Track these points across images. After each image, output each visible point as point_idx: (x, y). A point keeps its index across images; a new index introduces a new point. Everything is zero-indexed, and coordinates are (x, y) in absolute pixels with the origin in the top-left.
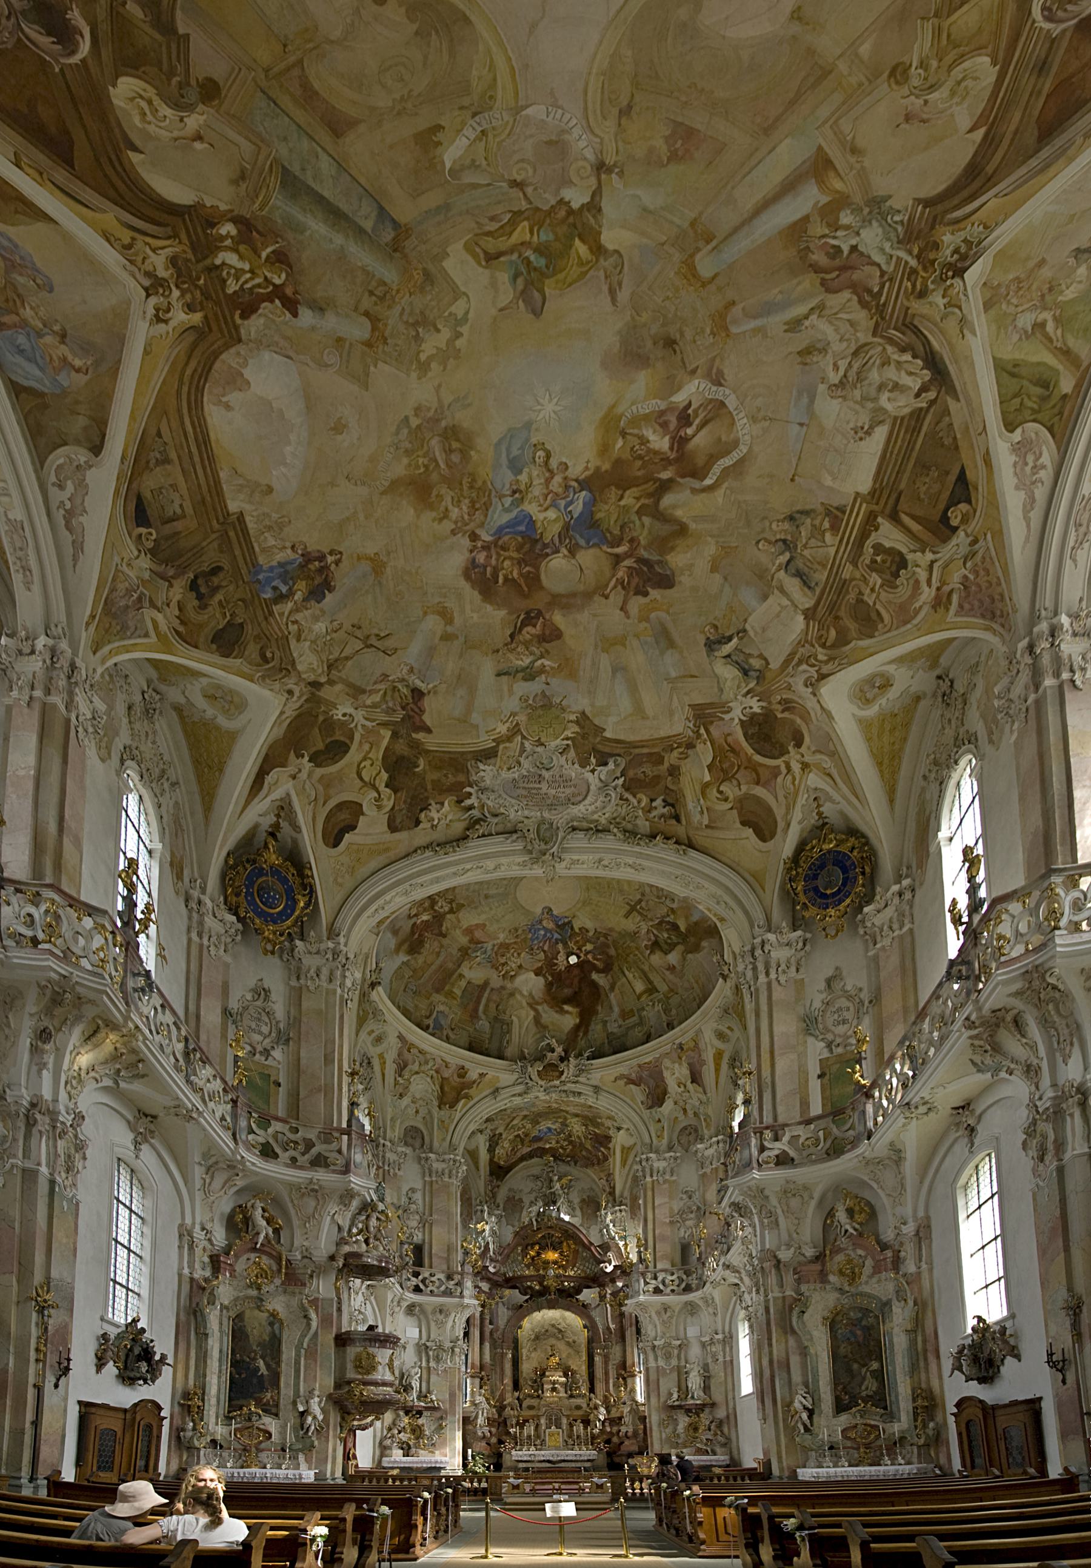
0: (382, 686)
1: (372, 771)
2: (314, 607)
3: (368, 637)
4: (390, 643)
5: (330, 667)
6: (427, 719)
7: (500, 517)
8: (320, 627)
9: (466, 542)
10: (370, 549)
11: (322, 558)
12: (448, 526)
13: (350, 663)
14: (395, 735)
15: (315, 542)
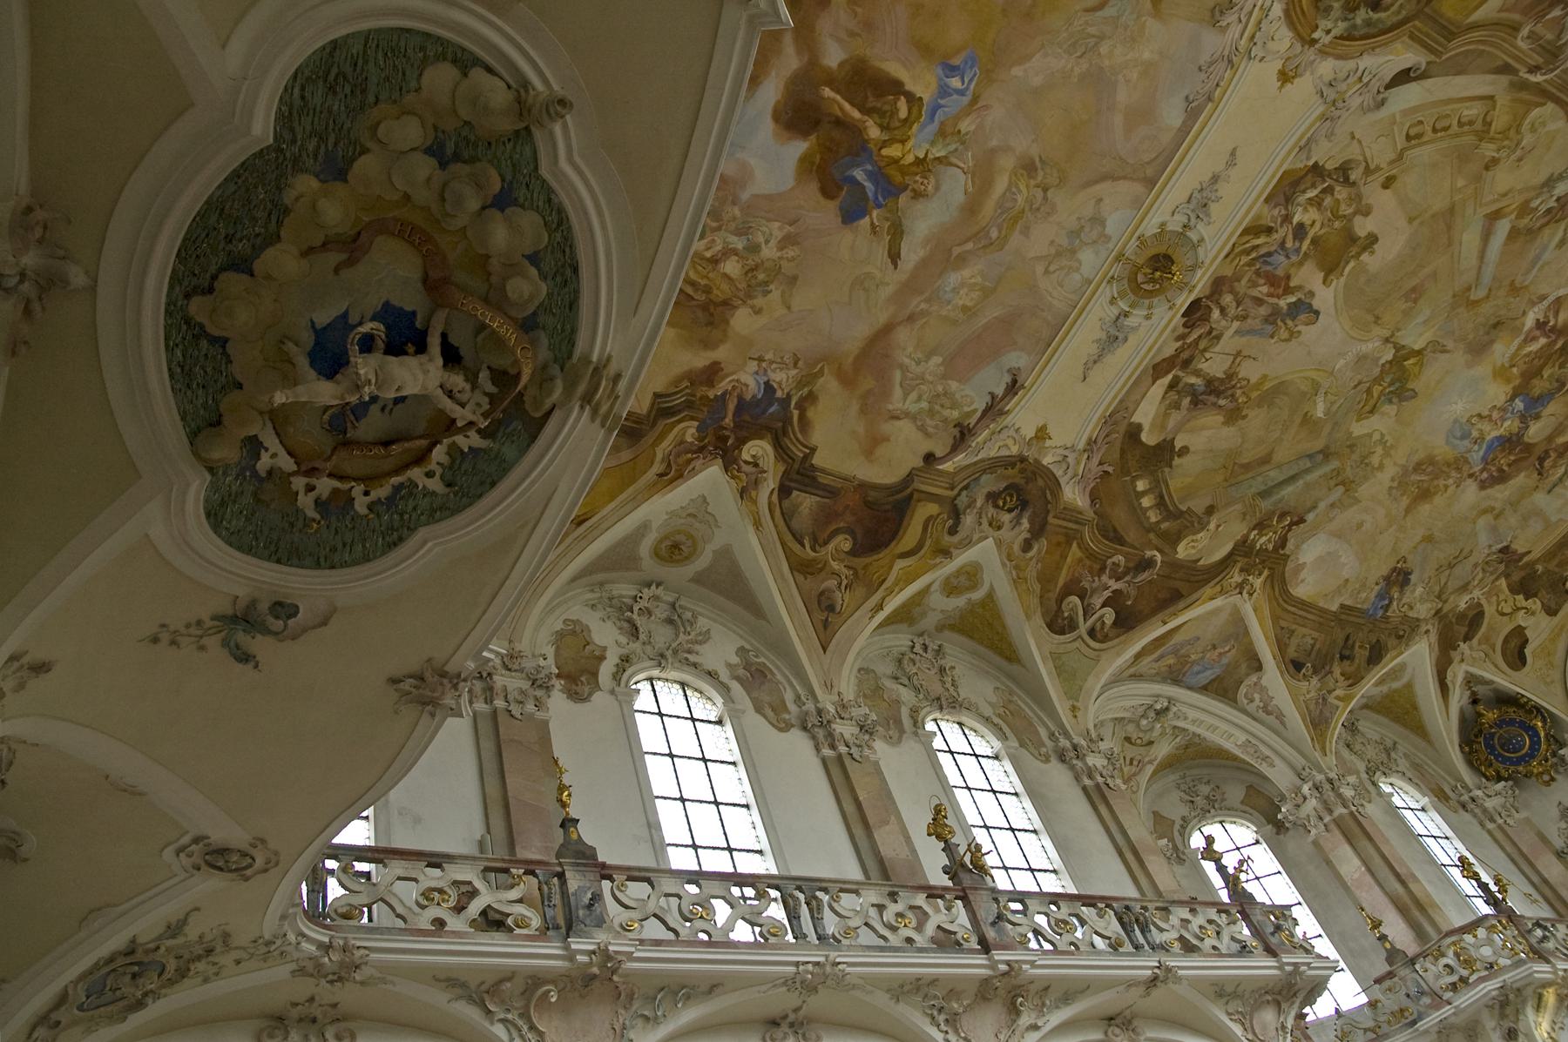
0: (1479, 569)
1: (1508, 601)
2: (1408, 589)
3: (1450, 564)
4: (1465, 553)
5: (1439, 597)
6: (1521, 550)
7: (1476, 456)
8: (1419, 590)
9: (1470, 481)
10: (1418, 538)
11: (1395, 569)
12: (1450, 490)
13: (1449, 583)
14: (1507, 576)
15: (1385, 571)
